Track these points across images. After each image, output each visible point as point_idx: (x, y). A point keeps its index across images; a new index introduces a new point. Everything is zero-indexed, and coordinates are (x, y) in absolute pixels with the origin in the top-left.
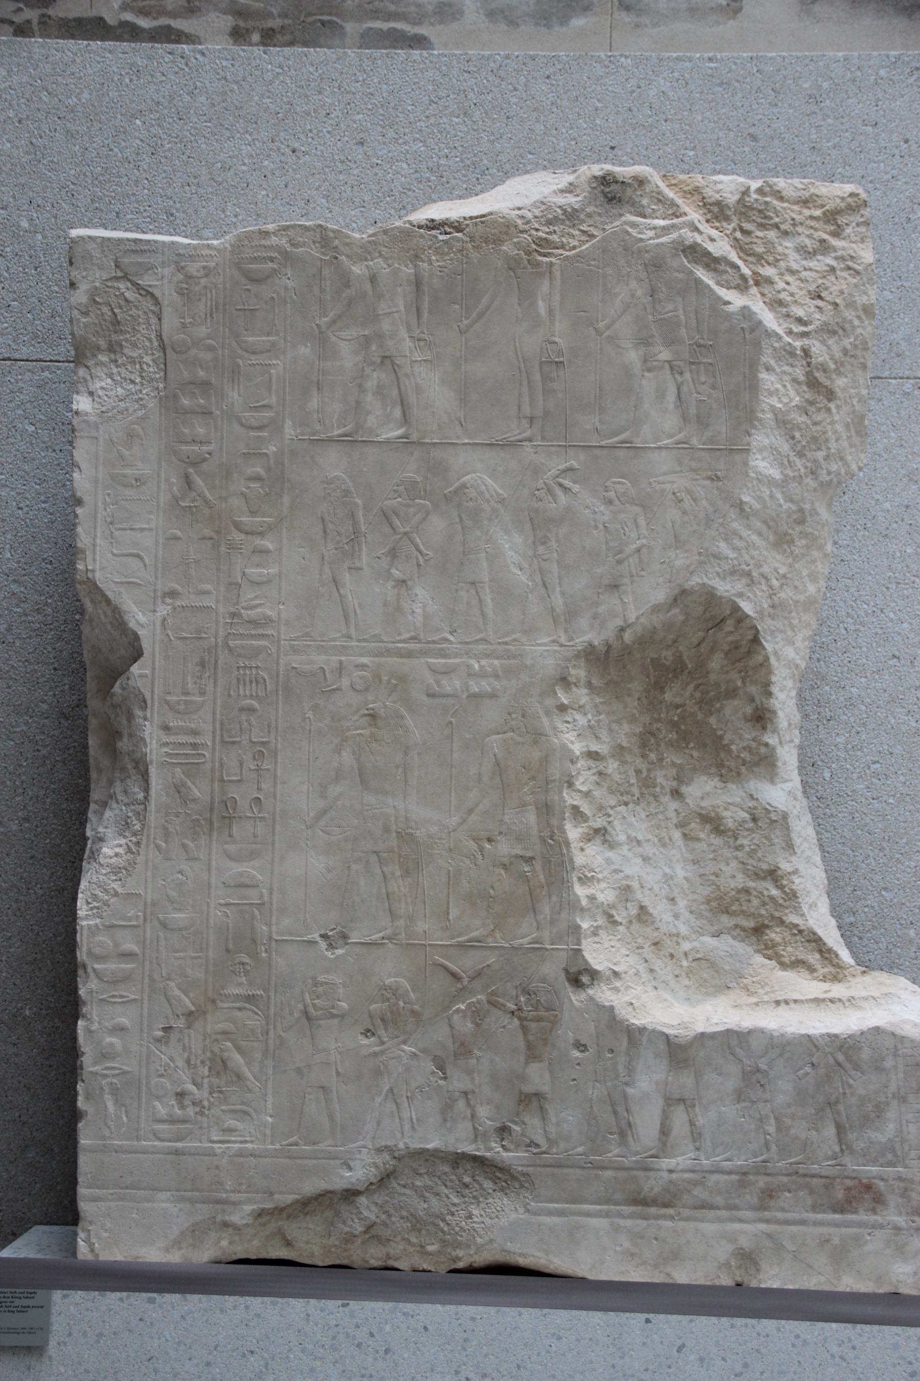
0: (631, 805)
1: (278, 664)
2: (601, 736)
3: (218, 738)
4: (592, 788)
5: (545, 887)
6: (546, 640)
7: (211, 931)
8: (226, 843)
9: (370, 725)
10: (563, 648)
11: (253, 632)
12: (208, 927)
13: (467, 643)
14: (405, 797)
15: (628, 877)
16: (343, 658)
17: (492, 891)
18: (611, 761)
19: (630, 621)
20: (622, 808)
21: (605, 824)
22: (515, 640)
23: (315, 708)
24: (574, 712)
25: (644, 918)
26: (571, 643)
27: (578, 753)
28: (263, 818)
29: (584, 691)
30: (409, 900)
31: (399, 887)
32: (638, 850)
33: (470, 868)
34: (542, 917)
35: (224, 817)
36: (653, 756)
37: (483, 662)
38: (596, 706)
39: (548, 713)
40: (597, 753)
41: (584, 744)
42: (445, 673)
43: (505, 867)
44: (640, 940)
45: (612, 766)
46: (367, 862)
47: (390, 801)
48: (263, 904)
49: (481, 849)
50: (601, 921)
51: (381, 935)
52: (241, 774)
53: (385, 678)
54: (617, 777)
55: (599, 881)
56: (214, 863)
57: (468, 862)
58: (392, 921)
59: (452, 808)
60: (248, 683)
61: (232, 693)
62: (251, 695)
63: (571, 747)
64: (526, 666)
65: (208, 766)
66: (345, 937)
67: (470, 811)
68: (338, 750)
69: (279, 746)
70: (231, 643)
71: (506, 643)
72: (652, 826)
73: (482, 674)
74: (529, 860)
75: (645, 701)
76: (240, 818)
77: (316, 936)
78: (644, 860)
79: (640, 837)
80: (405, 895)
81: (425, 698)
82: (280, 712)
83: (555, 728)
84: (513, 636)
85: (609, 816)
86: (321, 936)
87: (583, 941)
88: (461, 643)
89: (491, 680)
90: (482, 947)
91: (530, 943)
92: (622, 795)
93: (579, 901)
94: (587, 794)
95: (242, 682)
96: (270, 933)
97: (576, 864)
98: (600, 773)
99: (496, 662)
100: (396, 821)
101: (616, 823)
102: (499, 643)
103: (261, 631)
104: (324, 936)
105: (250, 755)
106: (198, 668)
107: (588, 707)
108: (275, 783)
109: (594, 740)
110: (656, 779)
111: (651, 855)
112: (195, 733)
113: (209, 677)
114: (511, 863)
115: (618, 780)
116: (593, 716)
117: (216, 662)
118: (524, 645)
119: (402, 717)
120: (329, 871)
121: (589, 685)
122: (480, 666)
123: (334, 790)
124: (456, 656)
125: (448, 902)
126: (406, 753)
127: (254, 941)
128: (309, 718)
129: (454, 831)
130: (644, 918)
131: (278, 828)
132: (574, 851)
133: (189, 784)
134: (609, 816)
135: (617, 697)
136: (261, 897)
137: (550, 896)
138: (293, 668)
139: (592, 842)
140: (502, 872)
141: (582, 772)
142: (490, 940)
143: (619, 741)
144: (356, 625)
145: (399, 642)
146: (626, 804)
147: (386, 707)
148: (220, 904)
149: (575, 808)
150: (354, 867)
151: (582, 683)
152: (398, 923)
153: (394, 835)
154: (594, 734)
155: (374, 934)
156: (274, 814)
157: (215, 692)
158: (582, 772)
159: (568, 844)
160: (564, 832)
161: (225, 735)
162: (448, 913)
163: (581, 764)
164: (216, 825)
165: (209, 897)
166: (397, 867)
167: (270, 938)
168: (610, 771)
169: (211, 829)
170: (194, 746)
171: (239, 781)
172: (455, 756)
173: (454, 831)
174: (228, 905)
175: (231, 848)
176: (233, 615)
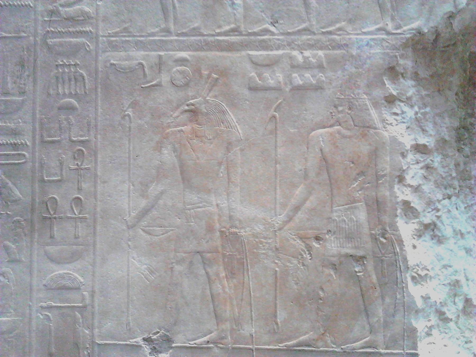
0: (454, 198)
1: (96, 61)
2: (427, 129)
3: (37, 137)
4: (421, 182)
5: (378, 288)
6: (373, 28)
7: (33, 335)
8: (48, 244)
9: (191, 121)
10: (390, 37)
11: (70, 30)
12: (30, 331)
13: (289, 34)
14: (228, 195)
15: (456, 271)
16: (162, 53)
17: (321, 293)
18: (436, 154)
19: (461, 6)
20: (446, 202)
21: (434, 219)
22: (340, 29)
23: (134, 105)
24: (402, 104)
25: (469, 310)
26: (399, 31)
27: (408, 147)
28: (85, 218)
29: (410, 83)
30: (235, 303)
31: (223, 287)
32: (461, 242)
33: (298, 269)
34: (376, 319)
35: (45, 218)
36: (467, 150)
37: (307, 53)
38: (422, 98)
39: (376, 105)
40: (425, 146)
41: (412, 137)
42: (268, 65)
43: (334, 266)
44: (467, 334)
45: (437, 160)
46: (191, 262)
47: (213, 199)
48: (85, 307)
49: (309, 248)
50: (434, 320)
51: (206, 339)
52: (62, 175)
53: (205, 73)
54: (441, 171)
55: (431, 278)
56: (35, 265)
57: (295, 262)
58: (218, 324)
59: (278, 206)
60: (67, 81)
61: (52, 92)
62: (71, 93)
63: (401, 139)
64: (352, 56)
65: (29, 166)
66: (168, 340)
67: (297, 209)
68: (159, 147)
69: (99, 144)
70: (49, 41)
71: (330, 33)
72: (469, 217)
73: (307, 66)
74: (360, 259)
75: (461, 96)
76: (61, 218)
77: (139, 340)
78: (467, 252)
79: (463, 231)
80: (230, 298)
81: (246, 92)
82: (100, 110)
83: (384, 121)
84: (338, 25)
85: (438, 210)
86: (144, 339)
87: (419, 344)
88: (282, 34)
89: (316, 71)
90: (312, 351)
91: (363, 348)
92: (445, 188)
93: (414, 302)
94: (416, 189)
95: (61, 80)
96: (93, 336)
97: (409, 263)
98: (427, 167)
99: (321, 53)
100: (219, 220)
101: (444, 218)
102: (323, 33)
103: (79, 28)
104: (147, 340)
105: (70, 154)
106: (18, 68)
107: (414, 99)
108: (95, 182)
109: (421, 133)
110: (471, 172)
111: (472, 247)
112: (14, 133)
113: (28, 76)
114: (341, 263)
115: (442, 173)
116: (420, 108)
117: (35, 60)
118: (349, 34)
119: (224, 112)
120: (152, 272)
121: (416, 76)
122: (303, 57)
123: (154, 189)
124: (278, 48)
125: (276, 305)
126: (228, 150)
127: (76, 345)
128: (129, 115)
129: (280, 229)
130: (469, 310)
131: (98, 228)
132: (406, 248)
133: (10, 185)
134: (438, 210)
135: (439, 91)
136: (83, 299)
137: (383, 299)
138: (112, 64)
139: (423, 238)
140: (332, 272)
141: (411, 166)
142: (320, 343)
143: (443, 134)
144: (175, 18)
145: (219, 34)
146: (449, 197)
147: (207, 102)
148: (42, 307)
149: (406, 204)
150: (178, 268)
151: (409, 75)
152: (224, 327)
153: (218, 234)
154: (421, 127)
155: (199, 338)
156: (95, 214)
157: (34, 91)
158: (411, 166)
159: (401, 242)
160: (396, 229)
161: (45, 135)
162: (275, 316)
163: (411, 157)
164: (37, 226)
165: (31, 300)
166: (221, 268)
167: (93, 342)
168: (436, 165)
169: (32, 231)
170: (15, 146)
171: (59, 181)
172: (279, 151)
173: (280, 229)
174: (50, 308)
175: (52, 249)
176: (52, 13)
